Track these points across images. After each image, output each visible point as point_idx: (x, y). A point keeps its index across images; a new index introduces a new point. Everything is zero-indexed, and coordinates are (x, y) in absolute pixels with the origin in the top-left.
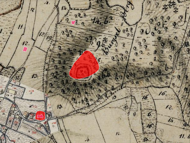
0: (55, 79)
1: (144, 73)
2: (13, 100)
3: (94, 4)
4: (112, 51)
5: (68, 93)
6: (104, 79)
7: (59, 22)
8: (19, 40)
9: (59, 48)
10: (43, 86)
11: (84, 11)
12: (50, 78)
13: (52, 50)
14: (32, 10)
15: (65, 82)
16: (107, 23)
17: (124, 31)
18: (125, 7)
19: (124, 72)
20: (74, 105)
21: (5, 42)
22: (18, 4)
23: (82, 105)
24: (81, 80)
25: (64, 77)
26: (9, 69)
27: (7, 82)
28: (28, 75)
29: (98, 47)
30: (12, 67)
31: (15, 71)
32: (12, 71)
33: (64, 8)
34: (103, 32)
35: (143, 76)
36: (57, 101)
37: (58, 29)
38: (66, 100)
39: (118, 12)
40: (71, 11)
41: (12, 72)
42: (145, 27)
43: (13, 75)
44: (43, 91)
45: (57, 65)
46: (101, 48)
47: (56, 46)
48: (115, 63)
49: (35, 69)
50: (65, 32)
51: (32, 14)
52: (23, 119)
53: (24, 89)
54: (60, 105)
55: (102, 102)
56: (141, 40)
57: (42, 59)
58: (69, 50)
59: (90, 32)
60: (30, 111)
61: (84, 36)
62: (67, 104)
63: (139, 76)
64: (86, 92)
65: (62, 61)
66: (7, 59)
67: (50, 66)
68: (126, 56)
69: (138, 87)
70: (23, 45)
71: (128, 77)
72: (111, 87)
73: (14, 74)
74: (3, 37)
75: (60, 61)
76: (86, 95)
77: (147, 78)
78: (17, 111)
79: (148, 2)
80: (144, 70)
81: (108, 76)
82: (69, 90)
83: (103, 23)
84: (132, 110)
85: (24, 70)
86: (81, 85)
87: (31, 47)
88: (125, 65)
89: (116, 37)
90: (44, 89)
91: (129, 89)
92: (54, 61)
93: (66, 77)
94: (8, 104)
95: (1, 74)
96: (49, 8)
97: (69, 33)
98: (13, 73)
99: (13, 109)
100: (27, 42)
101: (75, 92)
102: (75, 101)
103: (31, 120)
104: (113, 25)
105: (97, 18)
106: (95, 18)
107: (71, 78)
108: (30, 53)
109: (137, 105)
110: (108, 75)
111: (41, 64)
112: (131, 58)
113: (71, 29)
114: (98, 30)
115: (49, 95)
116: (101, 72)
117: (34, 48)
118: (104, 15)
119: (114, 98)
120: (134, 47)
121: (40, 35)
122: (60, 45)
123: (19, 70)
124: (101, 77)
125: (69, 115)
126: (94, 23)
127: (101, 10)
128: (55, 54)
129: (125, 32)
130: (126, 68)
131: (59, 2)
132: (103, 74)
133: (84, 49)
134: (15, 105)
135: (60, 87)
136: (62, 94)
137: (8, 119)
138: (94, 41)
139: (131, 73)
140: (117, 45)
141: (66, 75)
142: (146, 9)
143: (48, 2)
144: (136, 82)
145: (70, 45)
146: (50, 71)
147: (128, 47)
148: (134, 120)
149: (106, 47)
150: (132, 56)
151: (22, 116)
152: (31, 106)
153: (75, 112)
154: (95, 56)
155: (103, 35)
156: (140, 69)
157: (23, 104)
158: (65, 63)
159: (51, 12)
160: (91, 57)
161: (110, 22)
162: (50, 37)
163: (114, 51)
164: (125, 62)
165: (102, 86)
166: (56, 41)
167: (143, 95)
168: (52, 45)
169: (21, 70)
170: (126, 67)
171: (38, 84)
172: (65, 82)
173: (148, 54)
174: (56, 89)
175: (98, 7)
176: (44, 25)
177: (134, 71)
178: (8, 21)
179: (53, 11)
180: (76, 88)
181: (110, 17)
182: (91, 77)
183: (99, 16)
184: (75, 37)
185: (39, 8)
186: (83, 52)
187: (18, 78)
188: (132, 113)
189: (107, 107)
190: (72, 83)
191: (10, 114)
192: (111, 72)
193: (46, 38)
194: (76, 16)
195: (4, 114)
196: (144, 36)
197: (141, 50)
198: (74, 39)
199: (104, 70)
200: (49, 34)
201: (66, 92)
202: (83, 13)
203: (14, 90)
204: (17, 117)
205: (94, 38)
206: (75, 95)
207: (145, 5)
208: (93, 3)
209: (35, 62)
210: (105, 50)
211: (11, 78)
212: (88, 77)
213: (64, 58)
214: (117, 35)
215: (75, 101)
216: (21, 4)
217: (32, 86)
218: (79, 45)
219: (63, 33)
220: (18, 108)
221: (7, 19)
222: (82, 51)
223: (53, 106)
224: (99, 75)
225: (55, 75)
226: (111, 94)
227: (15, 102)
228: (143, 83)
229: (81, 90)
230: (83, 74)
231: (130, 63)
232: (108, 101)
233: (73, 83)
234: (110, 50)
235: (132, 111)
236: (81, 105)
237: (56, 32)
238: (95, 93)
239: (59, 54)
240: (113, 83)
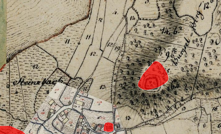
0: (123, 90)
1: (214, 84)
2: (80, 111)
3: (163, 14)
4: (181, 62)
5: (137, 104)
6: (174, 90)
7: (128, 32)
8: (87, 51)
9: (128, 58)
10: (111, 97)
11: (153, 21)
12: (118, 89)
13: (120, 61)
14: (101, 20)
15: (133, 93)
16: (176, 33)
17: (193, 42)
18: (195, 17)
19: (193, 83)
20: (143, 116)
21: (73, 53)
22: (86, 14)
23: (151, 117)
24: (150, 91)
25: (132, 88)
26: (77, 80)
27: (75, 93)
28: (96, 86)
29: (167, 58)
30: (79, 78)
31: (83, 82)
32: (80, 82)
33: (132, 18)
34: (172, 43)
35: (213, 87)
36: (126, 112)
37: (127, 40)
38: (135, 112)
39: (187, 22)
40: (139, 21)
41: (80, 83)
42: (215, 37)
43: (81, 86)
44: (111, 103)
45: (126, 76)
46: (170, 58)
47: (125, 57)
48: (185, 73)
49: (104, 80)
50: (133, 42)
51: (100, 24)
52: (90, 131)
53: (92, 100)
54: (129, 116)
55: (171, 114)
56: (211, 51)
57: (110, 70)
58: (138, 61)
59: (159, 42)
60: (98, 122)
61: (153, 46)
62: (135, 115)
63: (209, 87)
64: (155, 103)
65: (130, 72)
66: (75, 70)
67: (119, 76)
68: (195, 67)
69: (208, 98)
70: (91, 55)
71: (197, 88)
72: (180, 98)
73: (81, 85)
74: (71, 47)
75: (129, 72)
76: (155, 106)
77: (217, 89)
78: (85, 122)
79: (218, 12)
80: (214, 81)
81: (177, 87)
82: (138, 101)
83: (172, 33)
84: (201, 121)
85: (92, 81)
86: (150, 96)
87: (99, 57)
88: (194, 76)
89: (185, 47)
90: (112, 100)
91: (199, 100)
92: (122, 72)
93: (134, 88)
94: (76, 115)
95: (69, 85)
96: (118, 18)
97: (137, 43)
98: (81, 84)
99: (81, 120)
100: (95, 53)
101: (144, 103)
102: (144, 113)
103: (99, 131)
104: (182, 35)
105: (166, 29)
106: (164, 28)
107: (140, 89)
108: (98, 64)
109: (207, 116)
110: (177, 86)
111: (110, 75)
112: (201, 69)
113: (140, 39)
114: (167, 40)
115: (118, 106)
116: (171, 83)
117: (103, 59)
118: (173, 25)
119: (184, 109)
120: (204, 58)
121: (108, 45)
122: (129, 56)
123: (87, 81)
124: (170, 88)
125: (138, 126)
126: (163, 34)
127: (171, 20)
128: (123, 65)
129: (195, 42)
130: (195, 79)
131: (127, 12)
132: (172, 85)
133: (153, 60)
134: (83, 116)
135: (129, 98)
136: (130, 105)
137: (75, 130)
138: (163, 52)
139: (201, 84)
140: (186, 56)
141: (135, 86)
142: (216, 19)
143: (116, 12)
144: (206, 93)
145: (139, 56)
146: (119, 82)
147: (198, 58)
148: (203, 132)
149: (176, 57)
150: (202, 66)
151: (89, 127)
152: (100, 117)
153: (144, 124)
154: (164, 66)
155: (172, 45)
156: (210, 80)
157: (91, 115)
158: (134, 74)
159: (120, 22)
160: (160, 68)
161: (179, 32)
162: (119, 48)
163: (184, 62)
164: (195, 73)
165: (171, 98)
166: (124, 52)
167: (213, 106)
168: (120, 55)
169: (89, 81)
170: (196, 78)
171: (106, 95)
172: (133, 93)
173: (218, 65)
174: (124, 101)
175: (167, 17)
176: (112, 35)
177: (204, 82)
178: (75, 31)
179: (121, 21)
180: (145, 99)
181: (180, 27)
182: (160, 88)
183: (168, 27)
184: (144, 47)
185: (107, 19)
186: (152, 63)
187: (86, 89)
188: (201, 124)
189: (176, 119)
190: (141, 94)
191: (77, 126)
192: (180, 83)
193: (114, 48)
194: (145, 26)
195: (71, 125)
196: (214, 46)
197: (211, 60)
198: (143, 49)
199: (173, 81)
200: (117, 44)
201: (135, 103)
202: (152, 23)
203: (82, 101)
204: (85, 128)
205: (163, 48)
206: (143, 106)
207: (215, 15)
208: (162, 13)
209: (104, 73)
210: (174, 61)
211: (78, 89)
212: (157, 88)
213: (132, 68)
214: (186, 45)
215: (144, 113)
216: (89, 14)
217: (100, 97)
218: (148, 56)
219: (132, 43)
220: (86, 120)
221: (75, 29)
222: (151, 62)
223: (121, 117)
224: (169, 86)
225: (123, 86)
226: (181, 105)
227: (83, 114)
228: (213, 94)
229: (150, 101)
230: (152, 85)
231: (199, 73)
232: (178, 112)
233: (142, 94)
234: (179, 61)
235: (202, 123)
236: (150, 117)
237: (124, 43)
238: (164, 104)
239: (128, 65)
240: (182, 94)
